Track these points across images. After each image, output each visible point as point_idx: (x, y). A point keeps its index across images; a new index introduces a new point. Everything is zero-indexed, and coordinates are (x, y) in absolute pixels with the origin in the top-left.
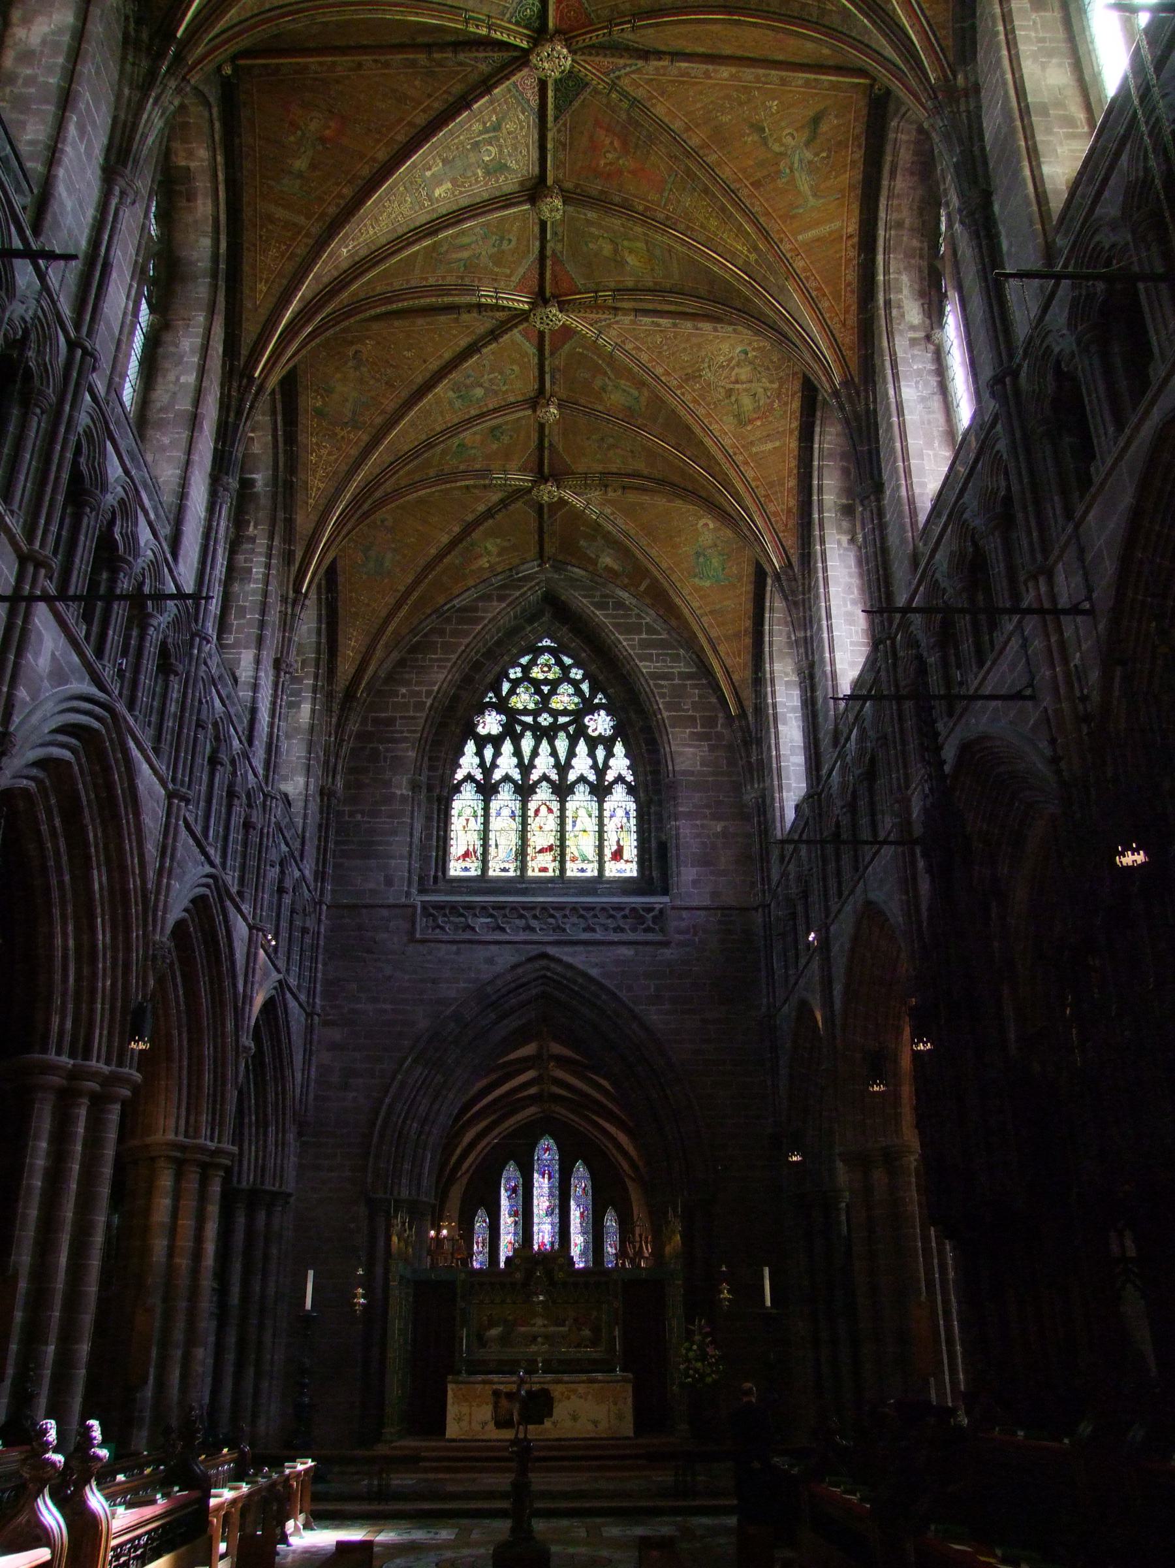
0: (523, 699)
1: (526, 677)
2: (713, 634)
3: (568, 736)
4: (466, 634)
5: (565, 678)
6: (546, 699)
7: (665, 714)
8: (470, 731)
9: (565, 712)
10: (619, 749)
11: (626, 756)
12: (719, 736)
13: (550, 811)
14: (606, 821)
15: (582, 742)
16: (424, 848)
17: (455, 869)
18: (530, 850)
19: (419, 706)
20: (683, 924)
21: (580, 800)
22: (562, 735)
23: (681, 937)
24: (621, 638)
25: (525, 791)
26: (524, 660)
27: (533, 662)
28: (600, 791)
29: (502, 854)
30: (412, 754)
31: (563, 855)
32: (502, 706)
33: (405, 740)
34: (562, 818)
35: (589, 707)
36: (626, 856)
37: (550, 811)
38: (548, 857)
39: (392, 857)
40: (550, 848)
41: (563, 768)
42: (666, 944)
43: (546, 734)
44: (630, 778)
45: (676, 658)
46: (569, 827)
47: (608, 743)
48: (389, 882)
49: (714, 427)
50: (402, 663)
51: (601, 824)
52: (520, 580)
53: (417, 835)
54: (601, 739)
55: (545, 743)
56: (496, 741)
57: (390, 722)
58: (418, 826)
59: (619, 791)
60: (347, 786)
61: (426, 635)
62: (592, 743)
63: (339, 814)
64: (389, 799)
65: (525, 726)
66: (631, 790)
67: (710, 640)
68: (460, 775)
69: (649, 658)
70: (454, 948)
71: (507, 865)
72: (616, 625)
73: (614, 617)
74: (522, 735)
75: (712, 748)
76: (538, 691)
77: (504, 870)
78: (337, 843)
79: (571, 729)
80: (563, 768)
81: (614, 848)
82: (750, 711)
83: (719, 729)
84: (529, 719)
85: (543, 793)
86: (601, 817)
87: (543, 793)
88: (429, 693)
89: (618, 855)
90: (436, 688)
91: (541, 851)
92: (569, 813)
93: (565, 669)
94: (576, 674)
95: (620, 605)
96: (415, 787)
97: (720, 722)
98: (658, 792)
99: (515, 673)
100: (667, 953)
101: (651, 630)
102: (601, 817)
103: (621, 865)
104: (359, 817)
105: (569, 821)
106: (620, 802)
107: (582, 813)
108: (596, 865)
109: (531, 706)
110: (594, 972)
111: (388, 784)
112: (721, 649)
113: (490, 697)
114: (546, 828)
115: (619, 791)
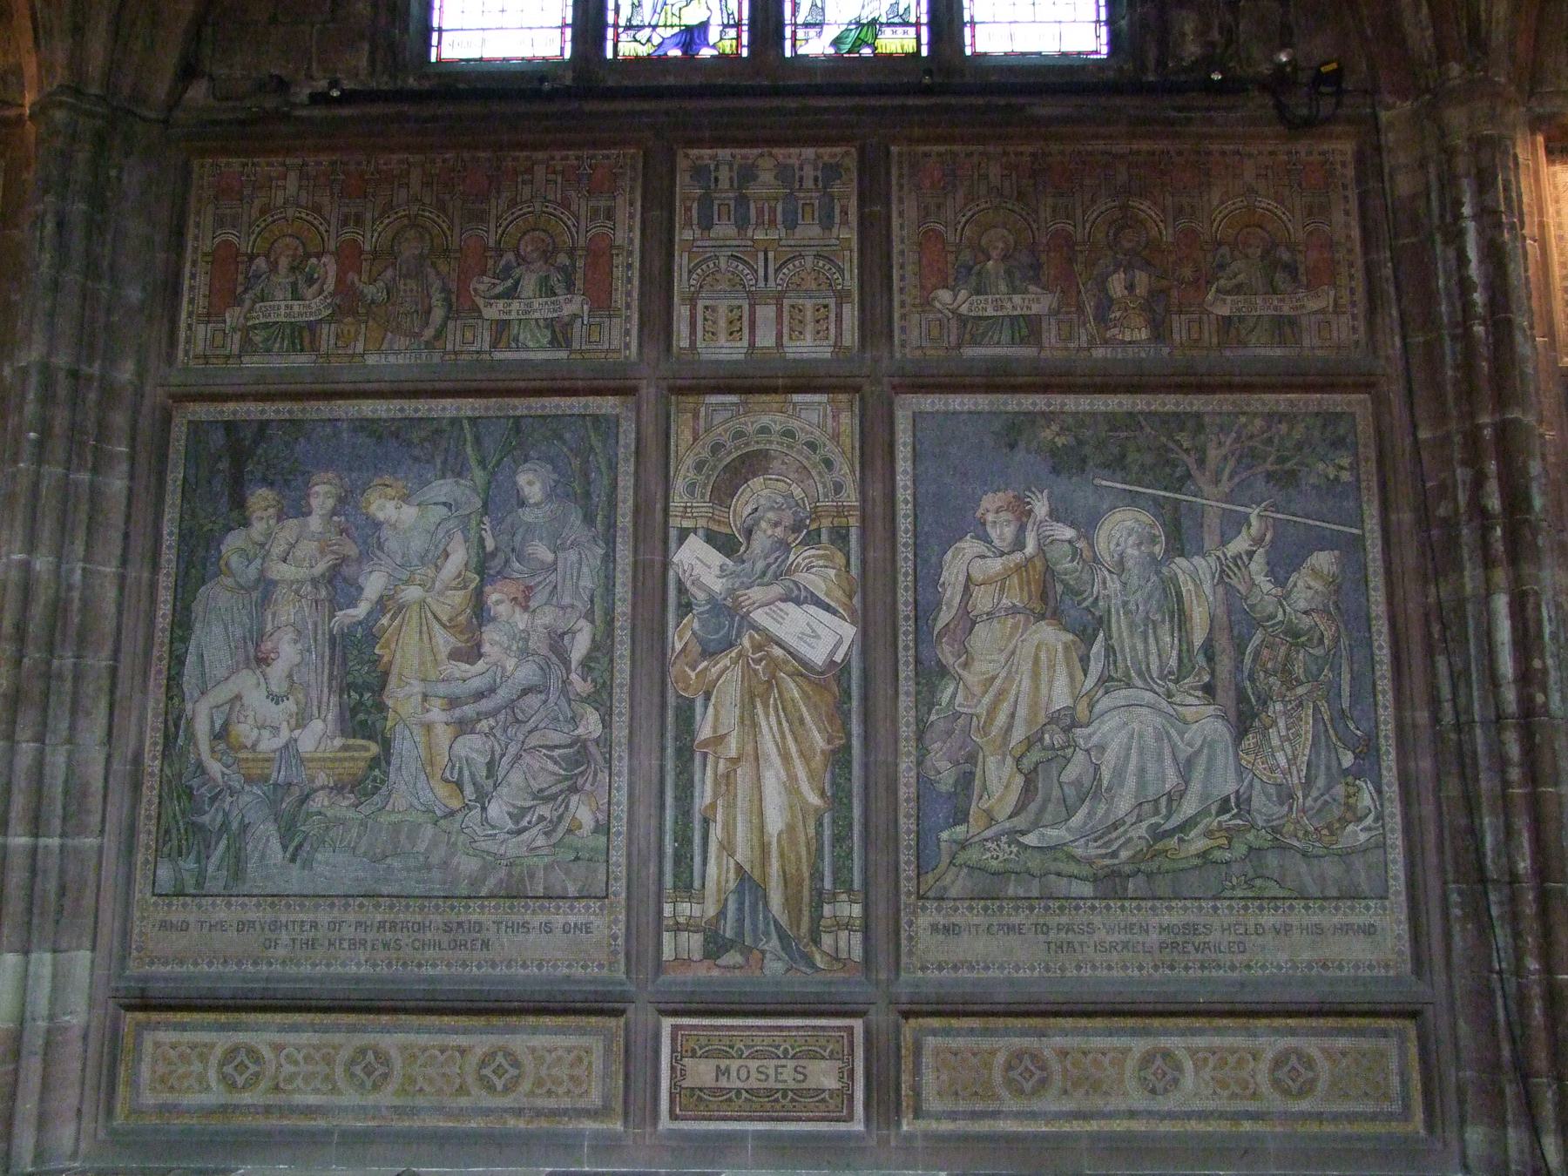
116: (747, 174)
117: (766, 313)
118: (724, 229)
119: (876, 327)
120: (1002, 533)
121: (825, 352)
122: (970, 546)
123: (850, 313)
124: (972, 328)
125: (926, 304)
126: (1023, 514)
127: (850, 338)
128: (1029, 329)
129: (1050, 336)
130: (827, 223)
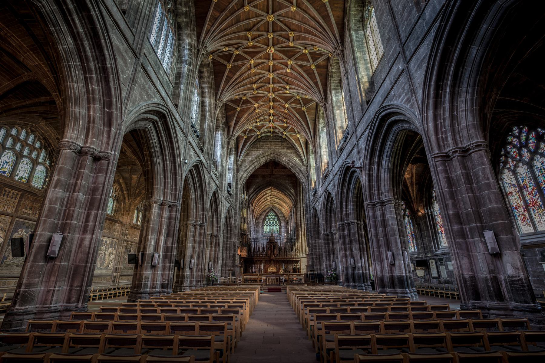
0: (270, 217)
25: (270, 226)
43: (272, 220)
59: (278, 226)
115: (278, 226)
116: (9, 192)
117: (6, 207)
118: (5, 197)
119: (16, 211)
120: (20, 233)
121: (10, 212)
122: (17, 233)
123: (14, 209)
124: (24, 213)
125: (21, 210)
126: (22, 231)
127: (13, 211)
128: (29, 214)
129: (30, 215)
130: (15, 199)
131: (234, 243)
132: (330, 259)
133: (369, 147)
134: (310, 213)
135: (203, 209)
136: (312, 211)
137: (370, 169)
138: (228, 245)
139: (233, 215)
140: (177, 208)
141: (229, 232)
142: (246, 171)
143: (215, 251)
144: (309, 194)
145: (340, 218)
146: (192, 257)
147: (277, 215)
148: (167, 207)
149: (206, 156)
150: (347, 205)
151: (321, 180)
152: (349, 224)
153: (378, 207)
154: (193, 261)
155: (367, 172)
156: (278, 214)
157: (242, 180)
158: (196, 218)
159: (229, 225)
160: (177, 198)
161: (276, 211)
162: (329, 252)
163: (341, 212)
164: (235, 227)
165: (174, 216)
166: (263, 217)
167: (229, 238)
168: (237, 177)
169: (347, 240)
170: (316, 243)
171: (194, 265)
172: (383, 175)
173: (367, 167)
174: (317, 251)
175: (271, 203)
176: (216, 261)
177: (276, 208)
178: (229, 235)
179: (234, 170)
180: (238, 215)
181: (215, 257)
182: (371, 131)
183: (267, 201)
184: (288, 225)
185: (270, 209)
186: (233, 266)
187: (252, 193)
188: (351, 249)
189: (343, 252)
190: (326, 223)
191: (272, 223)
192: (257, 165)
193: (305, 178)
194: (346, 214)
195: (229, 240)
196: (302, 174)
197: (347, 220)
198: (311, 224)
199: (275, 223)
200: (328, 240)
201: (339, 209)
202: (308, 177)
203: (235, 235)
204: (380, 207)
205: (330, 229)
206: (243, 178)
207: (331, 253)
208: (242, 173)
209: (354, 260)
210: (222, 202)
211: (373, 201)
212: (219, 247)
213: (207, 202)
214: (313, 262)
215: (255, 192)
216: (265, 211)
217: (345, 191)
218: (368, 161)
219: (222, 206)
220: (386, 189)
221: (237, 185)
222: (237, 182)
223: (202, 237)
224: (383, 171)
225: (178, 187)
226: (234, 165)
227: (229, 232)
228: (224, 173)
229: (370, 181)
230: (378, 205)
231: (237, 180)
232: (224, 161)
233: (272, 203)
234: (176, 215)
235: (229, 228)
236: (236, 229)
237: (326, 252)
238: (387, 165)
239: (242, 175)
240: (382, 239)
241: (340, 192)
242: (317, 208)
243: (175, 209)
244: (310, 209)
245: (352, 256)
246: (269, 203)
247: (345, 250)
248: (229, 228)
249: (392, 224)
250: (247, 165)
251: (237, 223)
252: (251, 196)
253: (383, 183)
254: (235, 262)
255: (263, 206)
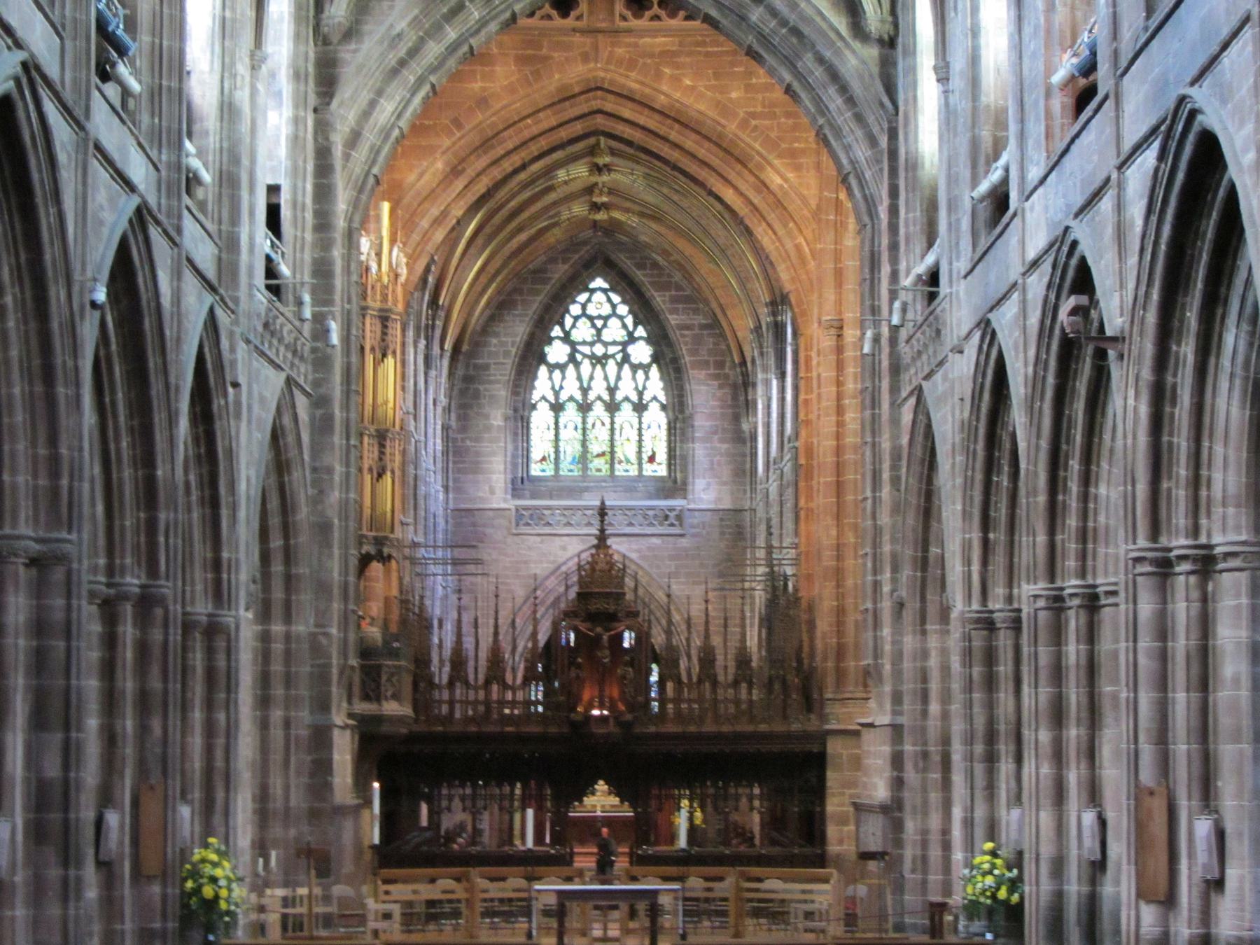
0: (583, 332)
1: (584, 314)
2: (722, 301)
3: (617, 363)
4: (537, 293)
5: (614, 314)
6: (599, 331)
7: (687, 359)
8: (542, 359)
9: (614, 343)
10: (654, 371)
11: (662, 378)
12: (726, 377)
13: (603, 424)
14: (644, 432)
15: (626, 367)
16: (514, 456)
17: (535, 470)
18: (589, 456)
19: (507, 354)
20: (695, 521)
21: (626, 414)
22: (611, 362)
23: (694, 531)
24: (656, 294)
25: (585, 408)
26: (582, 298)
27: (589, 300)
28: (640, 408)
29: (569, 459)
30: (503, 393)
31: (612, 458)
32: (566, 338)
33: (498, 382)
34: (612, 430)
35: (632, 339)
36: (658, 459)
37: (603, 424)
38: (602, 460)
39: (493, 473)
40: (603, 454)
41: (612, 391)
42: (682, 535)
44: (662, 398)
45: (696, 311)
46: (617, 437)
47: (646, 368)
48: (492, 492)
49: (712, 232)
50: (492, 318)
51: (640, 435)
52: (577, 244)
53: (509, 454)
54: (640, 366)
55: (599, 367)
56: (562, 367)
57: (486, 367)
58: (510, 447)
59: (654, 408)
60: (459, 418)
61: (510, 294)
62: (635, 368)
63: (455, 440)
64: (488, 428)
65: (585, 356)
66: (664, 407)
67: (721, 306)
68: (536, 396)
69: (674, 311)
70: (538, 539)
71: (572, 467)
72: (652, 283)
73: (652, 276)
74: (580, 363)
75: (721, 387)
76: (594, 326)
77: (570, 471)
78: (454, 463)
79: (619, 357)
80: (612, 391)
81: (650, 453)
82: (749, 360)
83: (727, 371)
84: (586, 350)
85: (599, 409)
86: (640, 429)
87: (599, 409)
88: (513, 343)
89: (652, 459)
90: (518, 339)
91: (598, 456)
92: (617, 426)
93: (614, 306)
94: (623, 309)
95: (655, 265)
96: (506, 419)
97: (728, 364)
98: (682, 411)
99: (575, 309)
100: (684, 542)
101: (679, 288)
102: (640, 429)
103: (654, 466)
104: (468, 443)
105: (617, 432)
106: (656, 419)
107: (626, 426)
108: (636, 467)
109: (589, 339)
110: (634, 556)
111: (487, 417)
112: (729, 313)
113: (557, 331)
114: (600, 439)
115: (654, 408)
131: (317, 649)
132: (991, 787)
133: (1156, 243)
134: (895, 421)
135: (149, 494)
136: (907, 416)
137: (1162, 360)
138: (277, 667)
139: (305, 437)
140: (69, 573)
141: (277, 568)
142: (394, 72)
143: (210, 730)
144: (894, 276)
145: (1041, 552)
146: (106, 798)
147: (644, 311)
148: (21, 569)
149: (145, 119)
150: (1087, 479)
151: (965, 224)
152: (1092, 603)
153: (1183, 582)
154: (112, 818)
155: (1147, 374)
156: (660, 300)
157: (361, 154)
158: (110, 553)
159: (275, 521)
160: (64, 510)
161: (640, 276)
162: (991, 737)
163: (1054, 512)
164: (324, 529)
165: (58, 616)
166: (516, 330)
167: (277, 610)
168: (323, 127)
169: (1074, 695)
170: (925, 654)
171: (121, 843)
172: (1221, 403)
173: (1149, 348)
174: (934, 708)
175: (596, 207)
176: (220, 795)
177: (636, 249)
178: (278, 594)
179: (297, 76)
180: (337, 439)
181: (209, 770)
182: (1166, 168)
183: (552, 197)
184: (750, 406)
185: (584, 252)
186: (314, 815)
187: (431, 196)
188: (1091, 753)
189: (1046, 770)
190: (986, 543)
191: (599, 388)
192: (483, 23)
193: (873, 141)
194: (1083, 535)
195: (277, 628)
196: (851, 101)
197: (1082, 574)
198: (896, 509)
199: (626, 388)
200: (990, 658)
201: (1042, 499)
202: (893, 134)
203: (323, 588)
204: (1193, 579)
205: (1010, 585)
206: (370, 137)
207: (1005, 748)
208: (365, 97)
209: (1102, 822)
210: (236, 385)
211: (1164, 541)
212: (230, 705)
213: (172, 441)
214: (898, 783)
215: (460, 184)
216: (539, 275)
217: (1082, 386)
218: (1152, 318)
219: (238, 416)
220: (1232, 489)
221: (323, 193)
222: (323, 168)
223: (155, 670)
224: (1224, 384)
225: (64, 451)
226: (297, 37)
227: (277, 568)
228: (245, 162)
229: (1157, 423)
230: (1185, 567)
231: (323, 155)
232: (242, 69)
233: (605, 206)
234: (69, 608)
235: (276, 543)
236: (326, 543)
237: (969, 740)
238: (1240, 359)
239: (366, 114)
240: (1182, 748)
241: (1049, 394)
242: (936, 418)
243: (58, 574)
244: (895, 389)
245: (1093, 794)
246: (579, 209)
247: (1058, 756)
248: (276, 543)
249: (1236, 681)
250: (402, 25)
251: (335, 496)
252: (425, 223)
253: (1219, 449)
254: (328, 786)
255: (523, 237)
